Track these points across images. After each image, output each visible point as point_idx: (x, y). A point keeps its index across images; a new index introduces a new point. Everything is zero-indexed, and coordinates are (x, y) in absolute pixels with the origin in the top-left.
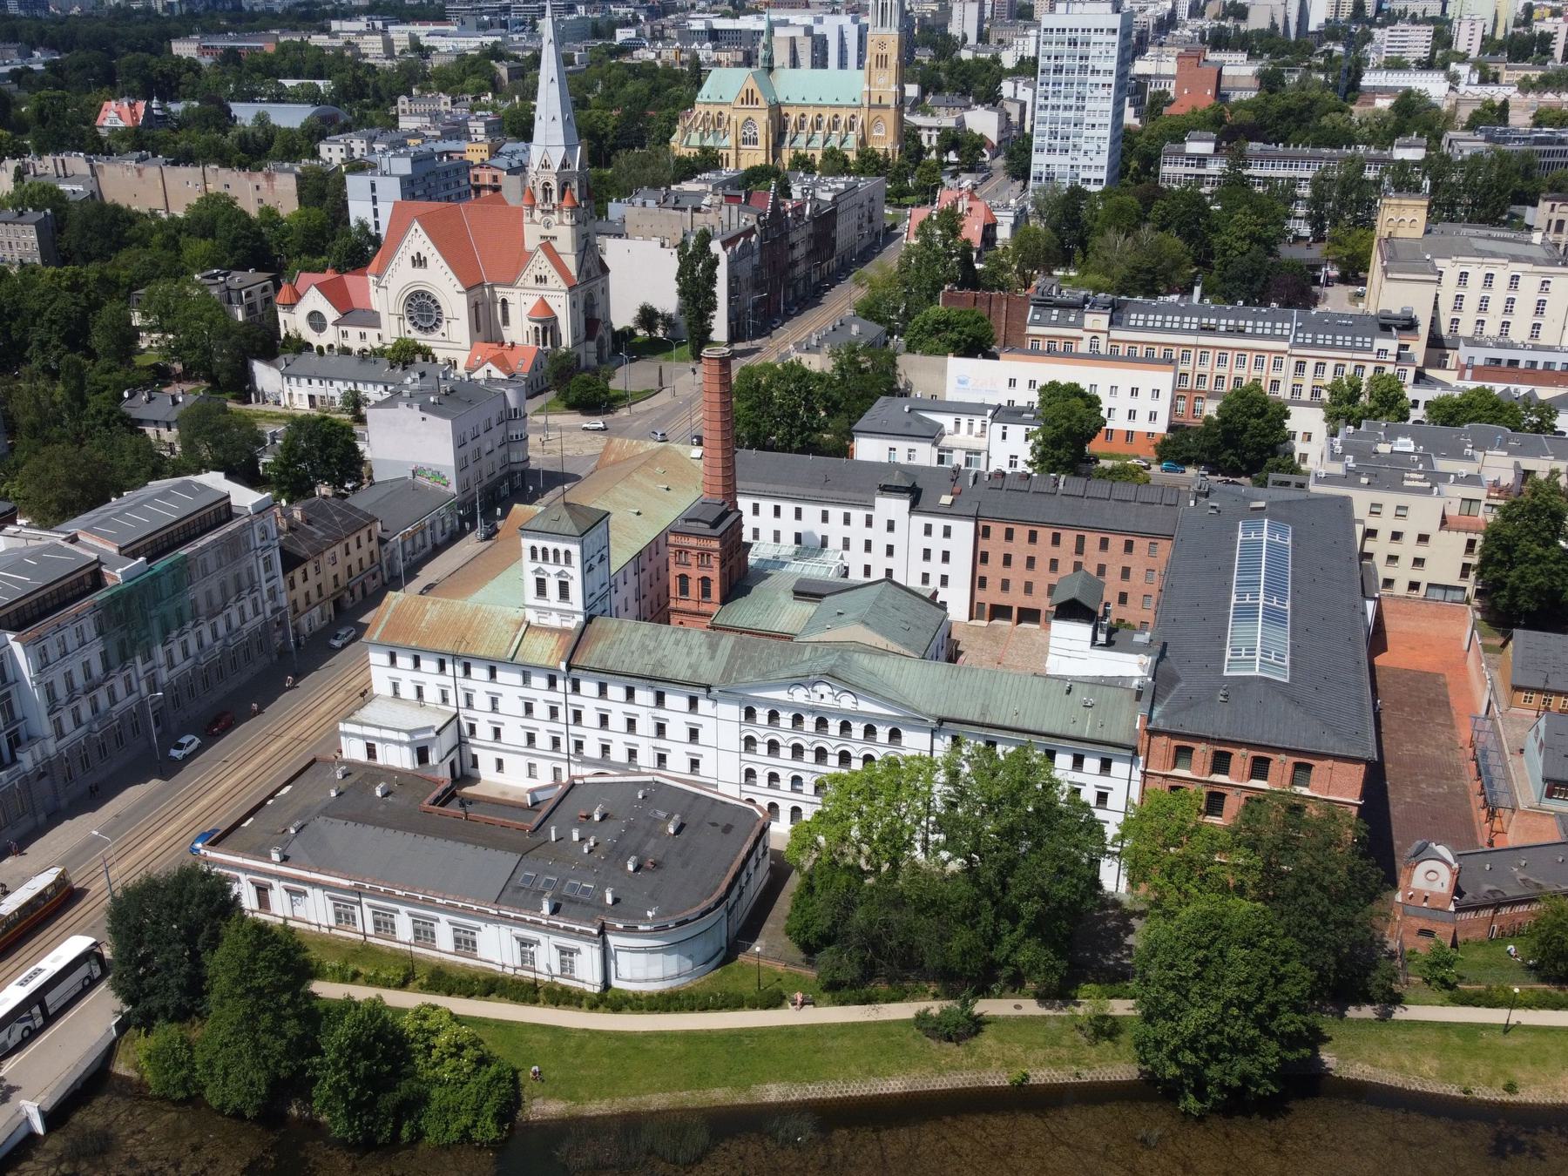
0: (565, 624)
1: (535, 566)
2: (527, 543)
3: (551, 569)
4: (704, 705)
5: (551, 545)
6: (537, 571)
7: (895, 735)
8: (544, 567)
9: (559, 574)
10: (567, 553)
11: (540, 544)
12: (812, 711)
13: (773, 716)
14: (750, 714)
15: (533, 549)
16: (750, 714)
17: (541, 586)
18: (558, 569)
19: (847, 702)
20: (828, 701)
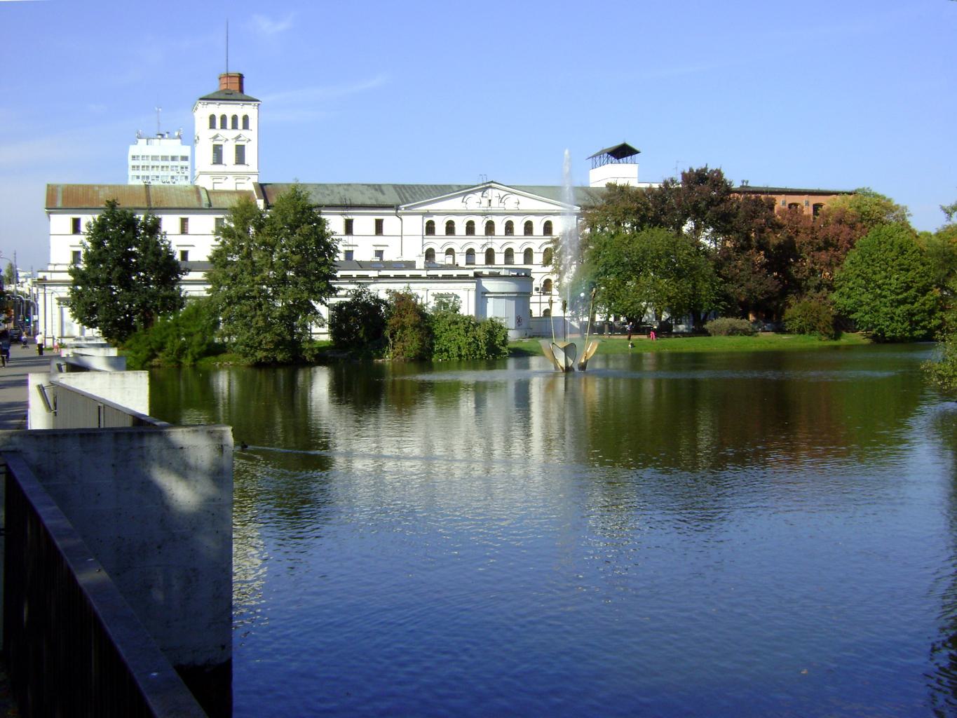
0: (240, 188)
1: (213, 133)
2: (203, 112)
3: (229, 134)
4: (390, 222)
5: (229, 109)
6: (215, 138)
7: (548, 228)
8: (223, 132)
9: (237, 138)
10: (246, 119)
11: (219, 109)
12: (484, 214)
13: (450, 228)
14: (430, 228)
15: (212, 118)
16: (430, 228)
17: (218, 152)
18: (235, 133)
19: (511, 203)
20: (496, 205)
